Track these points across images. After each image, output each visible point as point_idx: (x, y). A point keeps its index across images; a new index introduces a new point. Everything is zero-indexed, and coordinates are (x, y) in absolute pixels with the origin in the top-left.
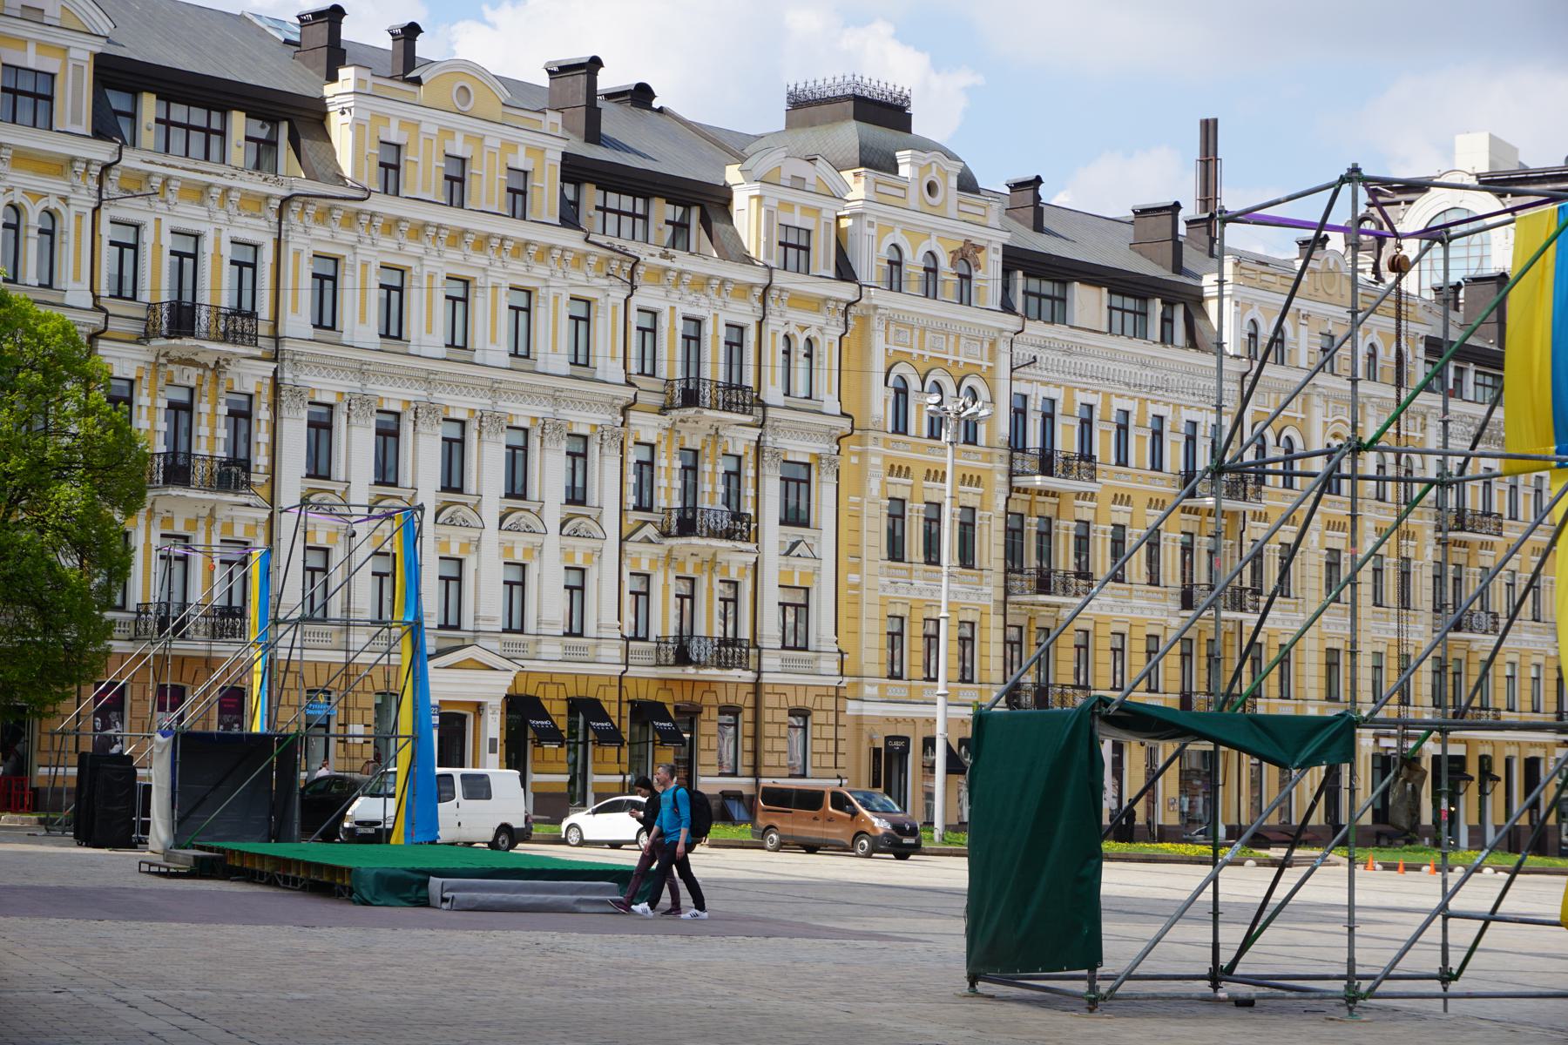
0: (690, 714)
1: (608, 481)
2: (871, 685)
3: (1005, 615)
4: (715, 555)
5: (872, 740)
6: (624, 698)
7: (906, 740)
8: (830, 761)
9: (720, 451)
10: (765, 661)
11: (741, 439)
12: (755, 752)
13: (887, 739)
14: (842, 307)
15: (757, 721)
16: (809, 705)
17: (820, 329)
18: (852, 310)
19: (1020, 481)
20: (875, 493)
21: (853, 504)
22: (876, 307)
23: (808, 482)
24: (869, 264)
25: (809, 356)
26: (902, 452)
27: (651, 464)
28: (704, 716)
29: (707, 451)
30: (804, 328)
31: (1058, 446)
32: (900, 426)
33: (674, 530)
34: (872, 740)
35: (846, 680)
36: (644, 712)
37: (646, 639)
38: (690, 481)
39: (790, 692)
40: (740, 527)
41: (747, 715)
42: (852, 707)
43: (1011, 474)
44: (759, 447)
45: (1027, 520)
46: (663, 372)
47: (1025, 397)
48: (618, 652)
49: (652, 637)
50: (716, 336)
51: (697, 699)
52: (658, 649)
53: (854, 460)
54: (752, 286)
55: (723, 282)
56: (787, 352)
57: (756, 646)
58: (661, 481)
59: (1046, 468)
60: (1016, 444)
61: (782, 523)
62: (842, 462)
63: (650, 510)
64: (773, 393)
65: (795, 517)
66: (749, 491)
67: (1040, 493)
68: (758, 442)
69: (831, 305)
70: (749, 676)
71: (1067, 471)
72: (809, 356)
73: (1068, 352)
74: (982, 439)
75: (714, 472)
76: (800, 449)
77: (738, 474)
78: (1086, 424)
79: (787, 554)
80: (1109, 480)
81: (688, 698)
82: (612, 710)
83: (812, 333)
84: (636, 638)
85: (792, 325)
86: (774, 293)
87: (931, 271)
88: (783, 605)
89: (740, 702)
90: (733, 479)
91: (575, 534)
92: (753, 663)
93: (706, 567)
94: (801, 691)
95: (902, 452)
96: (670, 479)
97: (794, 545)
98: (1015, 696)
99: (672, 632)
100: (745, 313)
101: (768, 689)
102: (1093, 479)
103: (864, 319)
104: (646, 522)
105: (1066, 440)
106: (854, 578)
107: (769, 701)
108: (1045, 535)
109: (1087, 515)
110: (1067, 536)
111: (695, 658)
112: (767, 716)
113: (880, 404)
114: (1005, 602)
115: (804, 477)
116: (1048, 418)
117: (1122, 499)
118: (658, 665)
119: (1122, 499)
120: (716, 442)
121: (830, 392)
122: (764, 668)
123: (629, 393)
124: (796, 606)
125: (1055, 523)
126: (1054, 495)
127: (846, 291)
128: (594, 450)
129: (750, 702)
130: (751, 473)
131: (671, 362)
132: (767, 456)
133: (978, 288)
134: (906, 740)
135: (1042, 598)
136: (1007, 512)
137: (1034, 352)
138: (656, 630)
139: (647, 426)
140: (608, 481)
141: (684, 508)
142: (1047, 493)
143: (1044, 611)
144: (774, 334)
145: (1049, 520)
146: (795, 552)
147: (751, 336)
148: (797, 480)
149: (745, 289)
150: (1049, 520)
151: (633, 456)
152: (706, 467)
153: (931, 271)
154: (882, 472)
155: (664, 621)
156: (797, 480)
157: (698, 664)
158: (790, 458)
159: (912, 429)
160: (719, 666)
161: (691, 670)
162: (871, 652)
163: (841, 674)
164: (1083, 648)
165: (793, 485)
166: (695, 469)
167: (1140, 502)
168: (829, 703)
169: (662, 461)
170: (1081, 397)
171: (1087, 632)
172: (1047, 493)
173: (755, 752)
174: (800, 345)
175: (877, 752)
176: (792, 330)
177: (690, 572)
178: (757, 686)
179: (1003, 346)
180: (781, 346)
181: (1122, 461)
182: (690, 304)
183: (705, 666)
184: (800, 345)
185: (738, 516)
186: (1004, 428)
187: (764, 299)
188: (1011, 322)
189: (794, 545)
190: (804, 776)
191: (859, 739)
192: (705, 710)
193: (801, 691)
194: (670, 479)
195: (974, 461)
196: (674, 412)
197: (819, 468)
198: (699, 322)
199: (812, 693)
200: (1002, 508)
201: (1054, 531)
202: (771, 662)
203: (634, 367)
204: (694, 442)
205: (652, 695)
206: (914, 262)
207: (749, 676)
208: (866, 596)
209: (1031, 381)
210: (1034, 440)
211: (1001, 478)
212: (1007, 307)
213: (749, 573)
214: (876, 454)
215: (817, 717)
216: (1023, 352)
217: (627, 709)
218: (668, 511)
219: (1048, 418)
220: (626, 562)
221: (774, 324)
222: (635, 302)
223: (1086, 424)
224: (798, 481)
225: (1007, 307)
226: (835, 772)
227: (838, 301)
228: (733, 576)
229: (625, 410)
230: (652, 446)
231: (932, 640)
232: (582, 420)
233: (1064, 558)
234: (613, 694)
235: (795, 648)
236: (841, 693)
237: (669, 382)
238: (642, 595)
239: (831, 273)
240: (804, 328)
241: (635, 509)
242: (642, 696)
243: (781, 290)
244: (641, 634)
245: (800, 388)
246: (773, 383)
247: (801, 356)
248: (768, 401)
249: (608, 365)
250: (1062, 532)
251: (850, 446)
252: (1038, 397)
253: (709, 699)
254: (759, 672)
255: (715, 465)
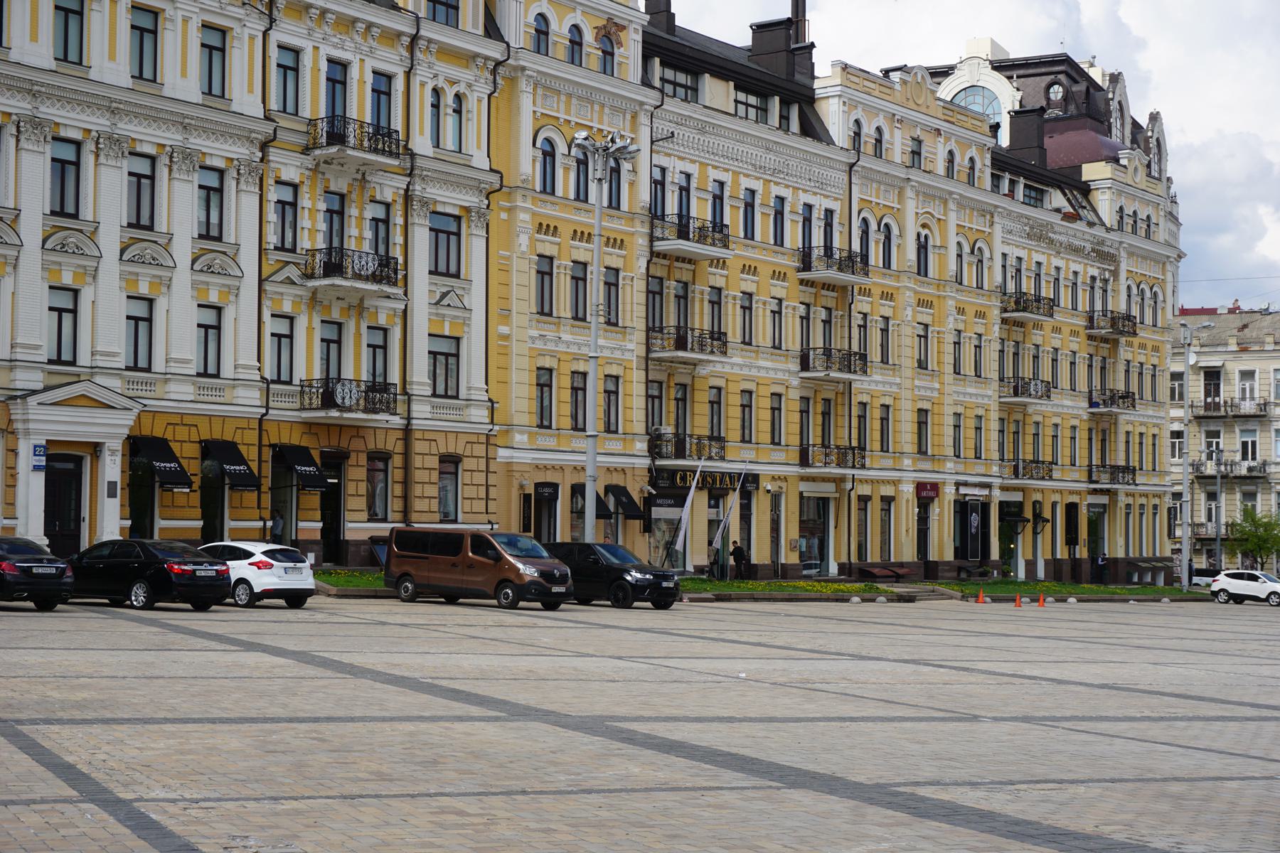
0: (336, 461)
1: (244, 216)
2: (522, 433)
3: (647, 370)
4: (362, 300)
5: (522, 487)
6: (265, 442)
7: (555, 486)
8: (480, 506)
9: (367, 197)
10: (415, 407)
11: (390, 188)
12: (406, 498)
13: (537, 485)
14: (491, 65)
15: (407, 467)
16: (460, 452)
17: (469, 86)
18: (501, 70)
19: (660, 246)
20: (524, 248)
21: (501, 258)
22: (523, 69)
23: (458, 235)
24: (517, 27)
25: (458, 111)
26: (550, 211)
27: (294, 205)
28: (352, 461)
29: (354, 196)
30: (453, 83)
31: (693, 213)
32: (548, 187)
33: (319, 270)
34: (522, 487)
35: (496, 428)
36: (285, 457)
37: (290, 383)
38: (336, 226)
39: (441, 439)
40: (388, 271)
41: (397, 461)
42: (502, 453)
43: (652, 238)
44: (408, 197)
45: (666, 283)
46: (306, 112)
47: (663, 170)
48: (257, 394)
49: (296, 381)
50: (362, 82)
51: (344, 444)
52: (302, 393)
53: (504, 216)
54: (399, 34)
55: (370, 26)
56: (436, 106)
57: (405, 393)
58: (305, 221)
59: (683, 233)
60: (656, 213)
61: (431, 273)
62: (492, 217)
63: (293, 250)
64: (421, 143)
65: (446, 269)
66: (398, 239)
67: (677, 259)
68: (407, 190)
69: (480, 61)
70: (397, 421)
71: (702, 239)
72: (458, 111)
73: (702, 131)
74: (625, 206)
75: (361, 218)
76: (451, 199)
77: (386, 221)
78: (718, 199)
79: (437, 303)
80: (737, 253)
81: (334, 442)
82: (251, 454)
83: (462, 88)
84: (279, 381)
85: (441, 79)
86: (422, 44)
87: (576, 43)
88: (433, 354)
89: (390, 447)
90: (382, 227)
91: (209, 270)
92: (401, 408)
93: (353, 312)
94: (451, 437)
95: (550, 211)
96: (314, 220)
97: (444, 295)
98: (657, 446)
99: (317, 374)
100: (392, 60)
101: (418, 435)
102: (726, 246)
103: (512, 81)
104: (288, 263)
105: (701, 210)
106: (504, 329)
107: (419, 447)
108: (683, 298)
109: (720, 282)
110: (702, 300)
111: (339, 401)
112: (417, 461)
113: (527, 164)
114: (647, 359)
115: (454, 229)
116: (685, 191)
117: (750, 269)
118: (302, 409)
119: (750, 269)
120: (363, 188)
121: (479, 147)
122: (414, 415)
123: (268, 128)
124: (447, 355)
125: (691, 288)
126: (690, 261)
127: (494, 51)
128: (230, 184)
129: (399, 448)
130: (400, 220)
131: (314, 102)
132: (416, 206)
133: (620, 64)
134: (555, 486)
135: (681, 354)
136: (648, 275)
137: (672, 127)
138: (300, 374)
139: (289, 167)
140: (244, 216)
141: (330, 249)
142: (684, 260)
143: (682, 369)
144: (423, 84)
145: (686, 284)
146: (445, 302)
147: (399, 85)
148: (447, 232)
149: (392, 37)
150: (686, 284)
151: (273, 194)
152: (353, 211)
153: (576, 43)
154: (531, 227)
155: (307, 363)
156: (447, 232)
157: (342, 408)
158: (440, 209)
159: (559, 191)
160: (366, 411)
161: (335, 413)
162: (520, 400)
163: (492, 422)
164: (716, 404)
165: (442, 237)
166: (341, 213)
167: (765, 271)
168: (480, 450)
169: (305, 201)
170: (714, 174)
171: (719, 389)
172: (684, 260)
173: (406, 498)
174: (448, 99)
175: (527, 498)
176: (441, 83)
177: (336, 315)
178: (407, 431)
179: (644, 119)
180: (429, 99)
181: (749, 233)
182: (335, 46)
183: (350, 410)
184: (448, 99)
185: (386, 261)
186: (645, 195)
187: (412, 47)
188: (651, 97)
189: (444, 295)
190: (455, 521)
191: (509, 485)
192: (353, 455)
193: (451, 437)
194: (314, 220)
195: (616, 226)
196: (318, 152)
197: (469, 220)
198: (344, 66)
199: (463, 439)
200: (643, 270)
201: (690, 295)
202: (421, 410)
203: (274, 104)
204: (340, 185)
205: (296, 438)
206: (560, 29)
207: (397, 421)
208: (515, 347)
209: (669, 155)
210: (672, 207)
211: (642, 242)
212: (646, 82)
213: (399, 321)
214: (525, 210)
215: (467, 464)
216: (663, 127)
217: (268, 454)
218: (312, 252)
219: (685, 191)
220: (267, 303)
221: (421, 74)
222: (275, 37)
223: (718, 199)
224: (449, 233)
225: (646, 82)
226: (485, 518)
227: (487, 58)
228: (382, 320)
229: (264, 146)
230: (295, 187)
231: (578, 390)
232: (218, 151)
233: (701, 319)
234: (252, 437)
235: (446, 396)
236: (492, 441)
237: (312, 122)
238: (285, 339)
239: (481, 31)
240: (453, 83)
241: (276, 248)
242: (285, 440)
243: (430, 41)
244: (284, 377)
245: (449, 141)
246: (422, 133)
247: (450, 111)
248: (416, 150)
249: (245, 98)
250: (698, 296)
251: (500, 200)
252: (677, 168)
253: (357, 444)
254: (409, 418)
255: (362, 210)
